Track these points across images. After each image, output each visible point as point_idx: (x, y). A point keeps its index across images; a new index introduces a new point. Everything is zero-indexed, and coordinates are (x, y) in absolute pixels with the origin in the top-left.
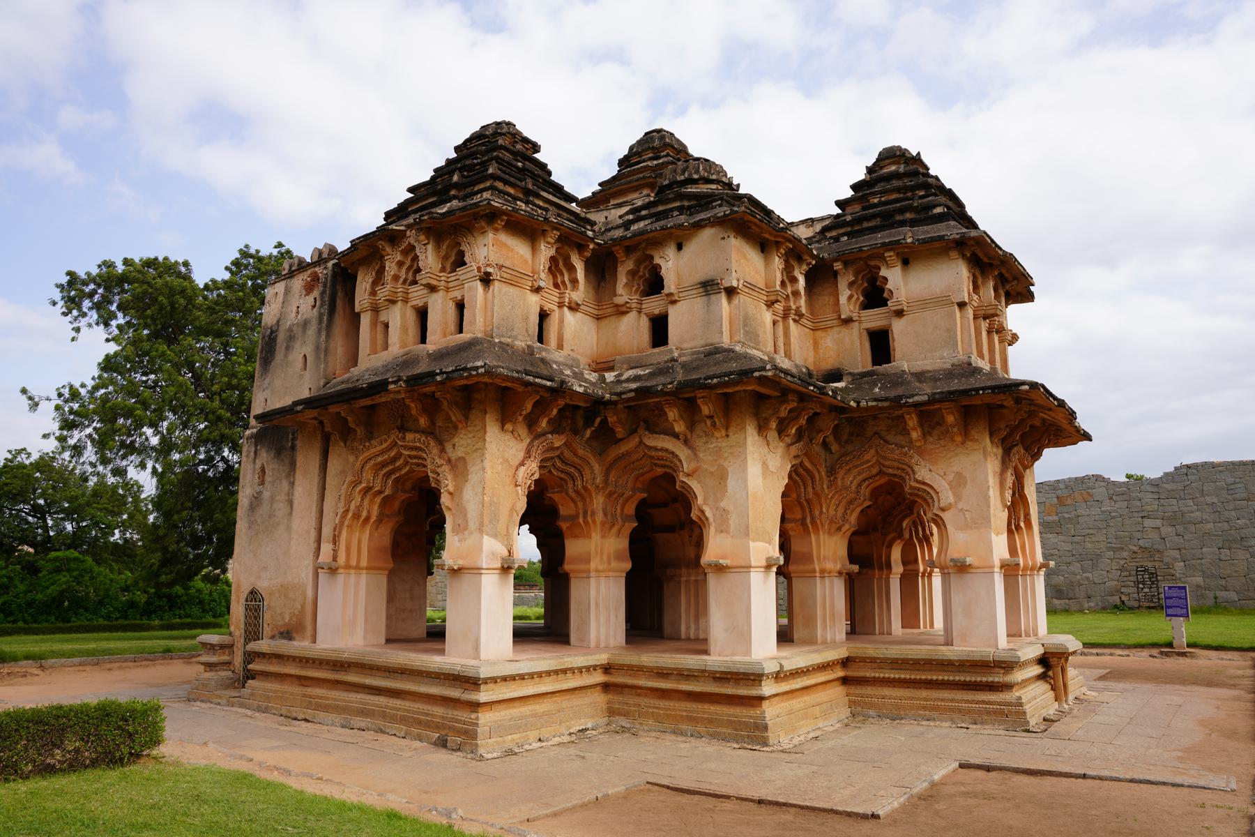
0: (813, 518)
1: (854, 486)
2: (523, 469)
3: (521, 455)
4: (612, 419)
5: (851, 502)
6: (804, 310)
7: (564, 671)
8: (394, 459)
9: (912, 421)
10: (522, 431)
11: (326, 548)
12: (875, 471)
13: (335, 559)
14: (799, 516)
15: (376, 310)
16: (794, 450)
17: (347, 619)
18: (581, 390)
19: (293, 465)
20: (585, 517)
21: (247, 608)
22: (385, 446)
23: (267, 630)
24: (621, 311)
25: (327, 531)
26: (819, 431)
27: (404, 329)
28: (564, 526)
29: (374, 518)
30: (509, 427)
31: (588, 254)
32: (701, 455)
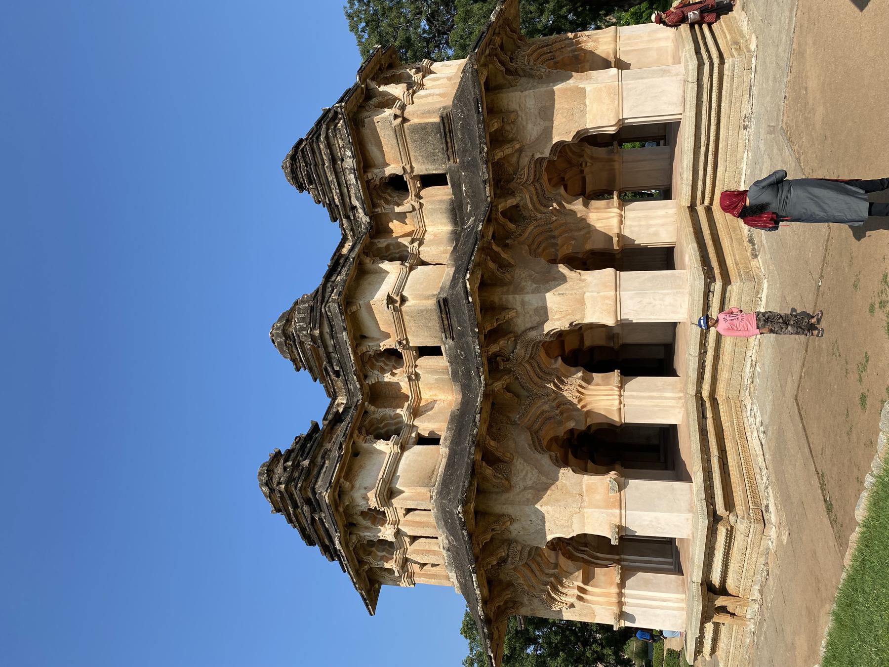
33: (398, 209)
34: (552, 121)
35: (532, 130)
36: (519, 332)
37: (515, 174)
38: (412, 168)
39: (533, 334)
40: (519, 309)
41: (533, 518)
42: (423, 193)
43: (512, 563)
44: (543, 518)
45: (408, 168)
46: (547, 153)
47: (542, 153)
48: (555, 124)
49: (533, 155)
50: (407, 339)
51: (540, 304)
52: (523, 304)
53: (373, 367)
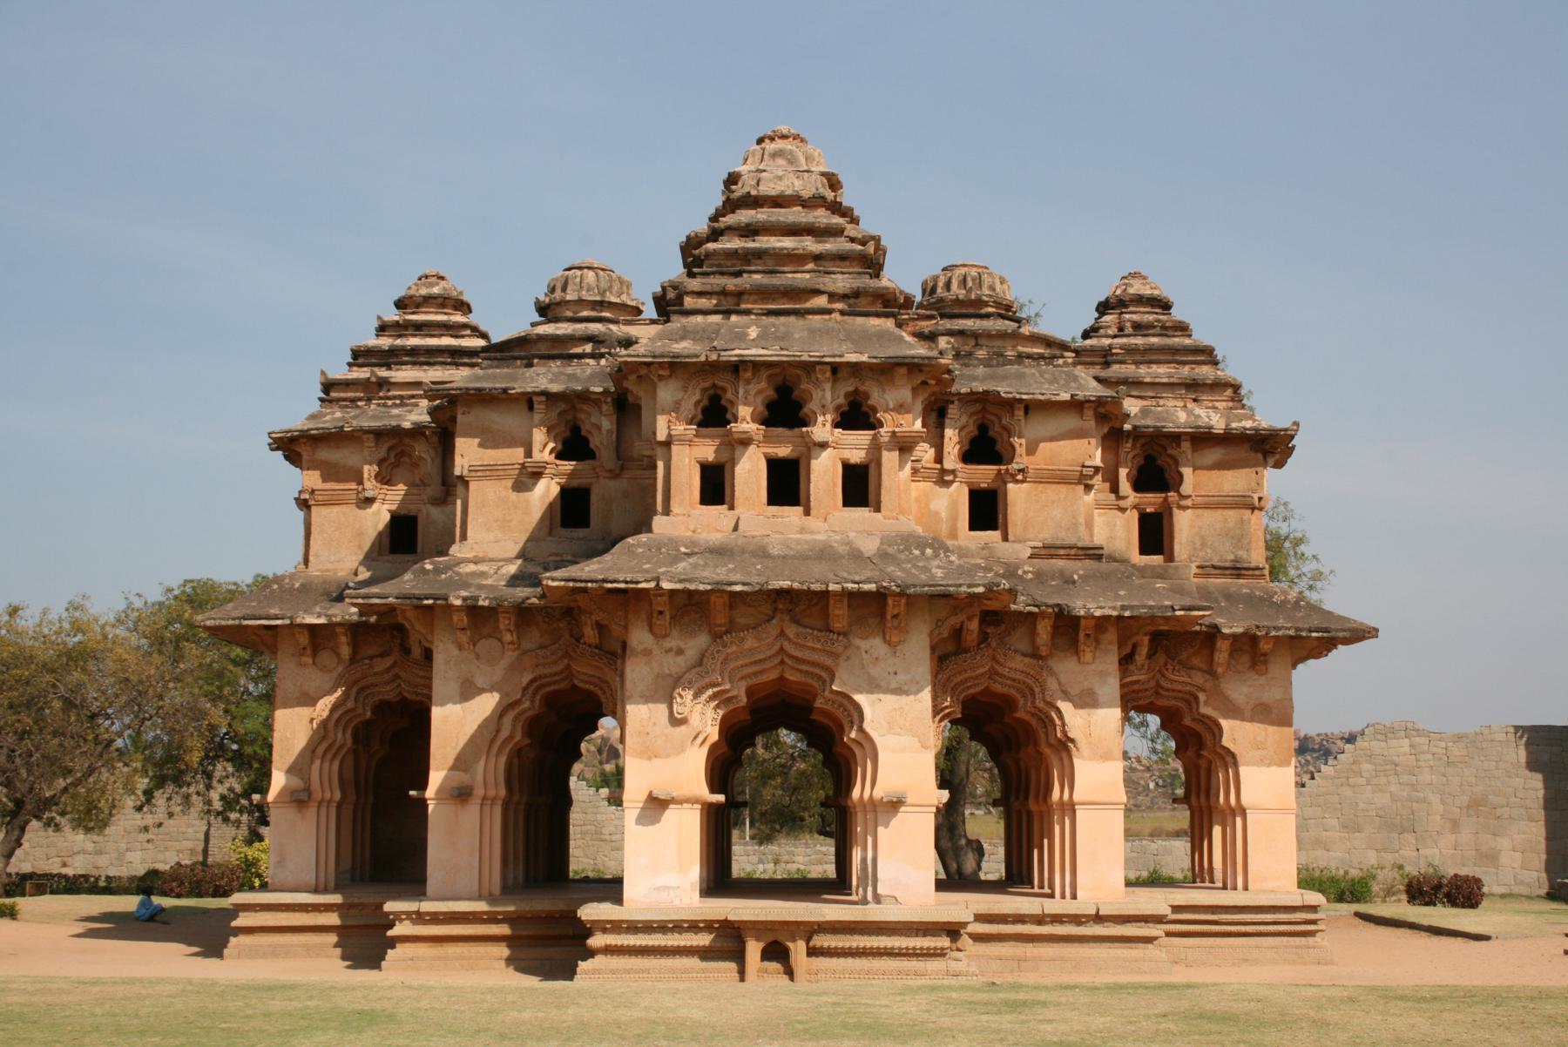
10: (326, 657)
18: (322, 621)
31: (435, 439)
33: (1123, 473)
34: (1252, 720)
35: (1240, 690)
36: (1051, 663)
37: (1180, 663)
38: (1185, 508)
39: (1052, 684)
40: (1093, 667)
41: (901, 677)
42: (1134, 516)
43: (798, 635)
44: (907, 693)
45: (1188, 502)
46: (1204, 710)
47: (1206, 703)
48: (1247, 725)
49: (1204, 691)
50: (1023, 481)
51: (1101, 699)
52: (1102, 674)
53: (971, 416)
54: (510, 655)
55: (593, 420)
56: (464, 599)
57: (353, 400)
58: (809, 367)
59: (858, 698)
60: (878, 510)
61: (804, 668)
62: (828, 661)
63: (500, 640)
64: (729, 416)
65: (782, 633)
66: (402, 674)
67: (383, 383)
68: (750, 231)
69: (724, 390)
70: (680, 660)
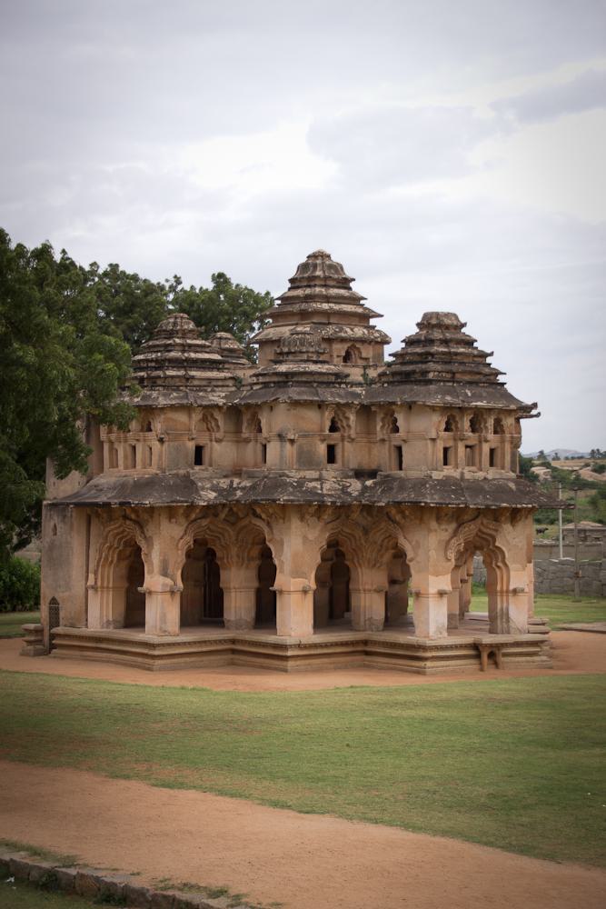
0: (358, 558)
1: (379, 542)
2: (182, 541)
3: (181, 534)
4: (235, 509)
5: (379, 551)
6: (353, 437)
7: (205, 642)
8: (124, 531)
9: (393, 511)
10: (182, 520)
11: (91, 576)
12: (388, 535)
13: (96, 583)
14: (351, 557)
15: (111, 443)
16: (330, 526)
17: (100, 614)
19: (71, 527)
20: (228, 558)
21: (50, 608)
22: (117, 525)
23: (61, 622)
24: (247, 441)
25: (92, 567)
26: (353, 512)
27: (126, 457)
28: (219, 563)
29: (115, 562)
30: (173, 520)
32: (274, 531)
54: (321, 524)
55: (347, 415)
56: (332, 502)
57: (178, 387)
58: (490, 410)
59: (504, 549)
60: (503, 468)
61: (484, 536)
62: (493, 533)
63: (319, 518)
64: (453, 427)
65: (482, 523)
66: (212, 527)
67: (188, 379)
68: (445, 342)
69: (454, 417)
70: (447, 533)
